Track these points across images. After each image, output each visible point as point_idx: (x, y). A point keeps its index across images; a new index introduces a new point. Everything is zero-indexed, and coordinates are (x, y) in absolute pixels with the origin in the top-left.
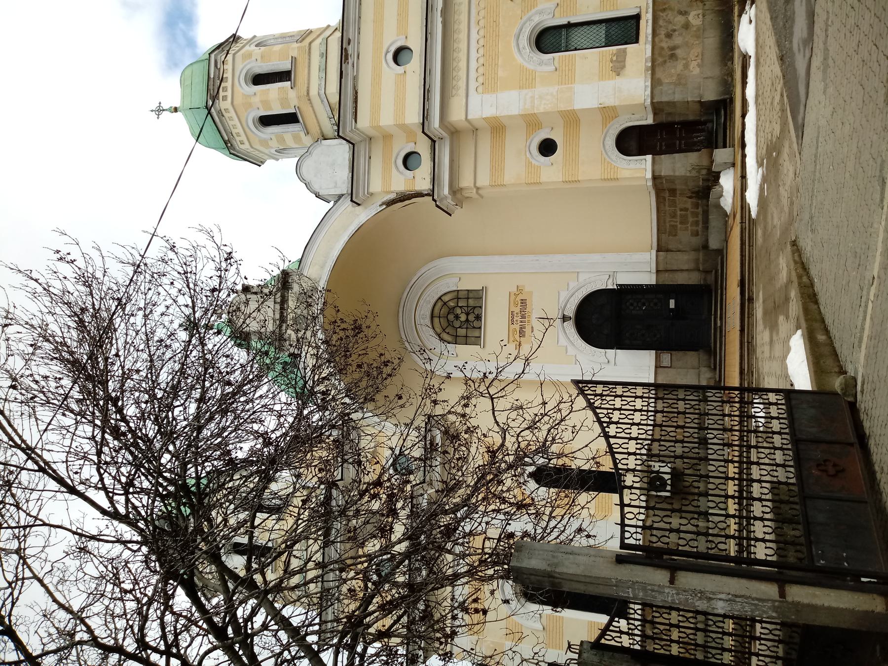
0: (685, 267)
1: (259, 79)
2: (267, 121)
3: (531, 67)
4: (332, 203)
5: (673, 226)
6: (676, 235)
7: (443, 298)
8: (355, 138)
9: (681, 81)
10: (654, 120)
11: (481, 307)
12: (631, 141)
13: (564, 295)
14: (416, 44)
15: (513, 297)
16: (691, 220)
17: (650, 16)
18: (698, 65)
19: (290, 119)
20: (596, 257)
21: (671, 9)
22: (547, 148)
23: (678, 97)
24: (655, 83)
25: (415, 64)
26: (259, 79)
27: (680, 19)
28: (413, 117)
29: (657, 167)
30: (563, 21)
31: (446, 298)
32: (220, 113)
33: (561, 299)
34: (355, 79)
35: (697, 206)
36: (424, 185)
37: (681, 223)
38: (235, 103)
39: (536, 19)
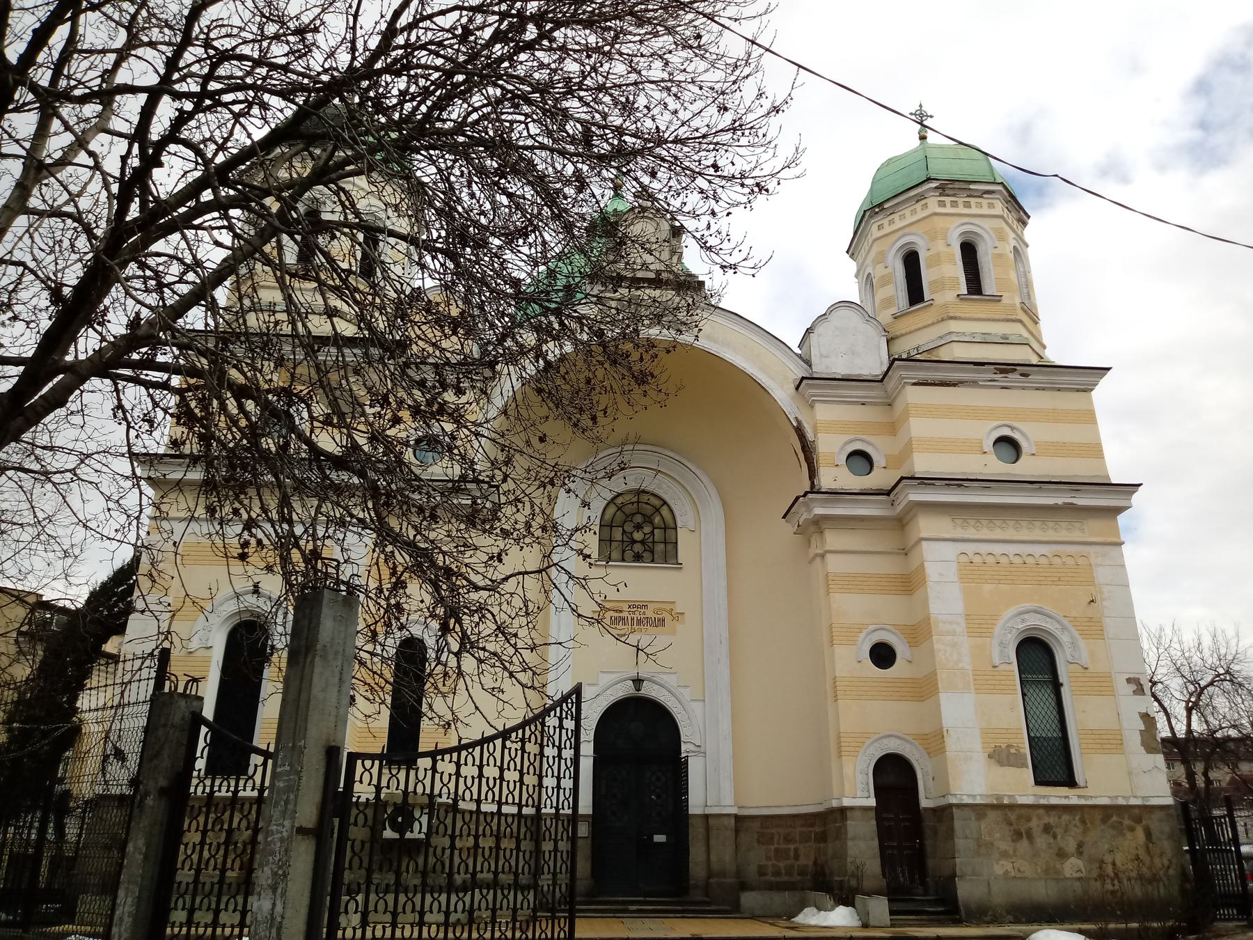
0: (713, 858)
1: (969, 251)
2: (911, 261)
3: (997, 630)
4: (798, 351)
5: (772, 838)
6: (759, 842)
7: (665, 507)
8: (891, 383)
9: (983, 847)
10: (925, 809)
11: (653, 561)
12: (894, 775)
13: (670, 680)
14: (1025, 468)
15: (668, 607)
16: (782, 864)
17: (1074, 801)
18: (1006, 872)
19: (915, 293)
20: (725, 725)
21: (1085, 832)
22: (883, 655)
23: (960, 843)
24: (979, 810)
25: (995, 466)
26: (969, 251)
27: (1071, 845)
28: (923, 464)
29: (858, 814)
30: (1063, 678)
31: (665, 511)
32: (921, 197)
33: (664, 677)
34: (974, 384)
35: (802, 872)
36: (827, 479)
37: (777, 850)
38: (936, 218)
39: (1065, 638)
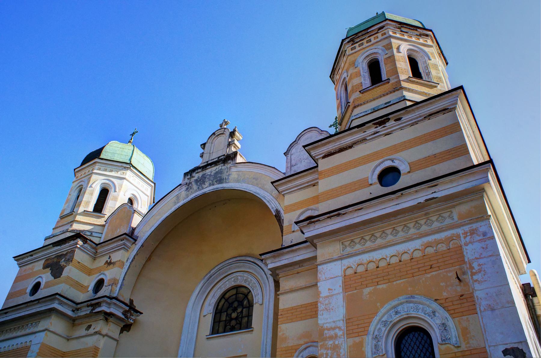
3: (372, 328)
25: (378, 189)
34: (364, 140)
